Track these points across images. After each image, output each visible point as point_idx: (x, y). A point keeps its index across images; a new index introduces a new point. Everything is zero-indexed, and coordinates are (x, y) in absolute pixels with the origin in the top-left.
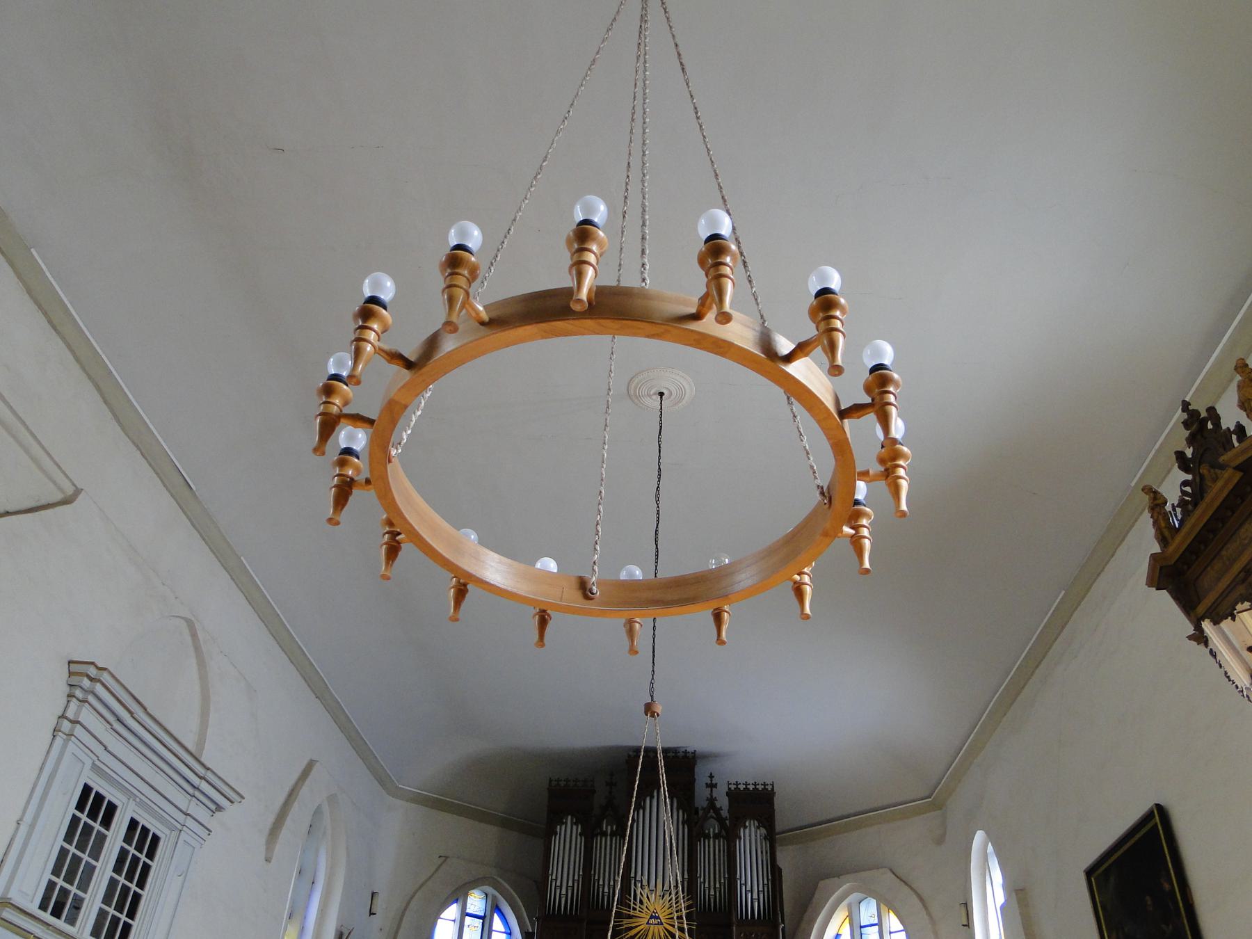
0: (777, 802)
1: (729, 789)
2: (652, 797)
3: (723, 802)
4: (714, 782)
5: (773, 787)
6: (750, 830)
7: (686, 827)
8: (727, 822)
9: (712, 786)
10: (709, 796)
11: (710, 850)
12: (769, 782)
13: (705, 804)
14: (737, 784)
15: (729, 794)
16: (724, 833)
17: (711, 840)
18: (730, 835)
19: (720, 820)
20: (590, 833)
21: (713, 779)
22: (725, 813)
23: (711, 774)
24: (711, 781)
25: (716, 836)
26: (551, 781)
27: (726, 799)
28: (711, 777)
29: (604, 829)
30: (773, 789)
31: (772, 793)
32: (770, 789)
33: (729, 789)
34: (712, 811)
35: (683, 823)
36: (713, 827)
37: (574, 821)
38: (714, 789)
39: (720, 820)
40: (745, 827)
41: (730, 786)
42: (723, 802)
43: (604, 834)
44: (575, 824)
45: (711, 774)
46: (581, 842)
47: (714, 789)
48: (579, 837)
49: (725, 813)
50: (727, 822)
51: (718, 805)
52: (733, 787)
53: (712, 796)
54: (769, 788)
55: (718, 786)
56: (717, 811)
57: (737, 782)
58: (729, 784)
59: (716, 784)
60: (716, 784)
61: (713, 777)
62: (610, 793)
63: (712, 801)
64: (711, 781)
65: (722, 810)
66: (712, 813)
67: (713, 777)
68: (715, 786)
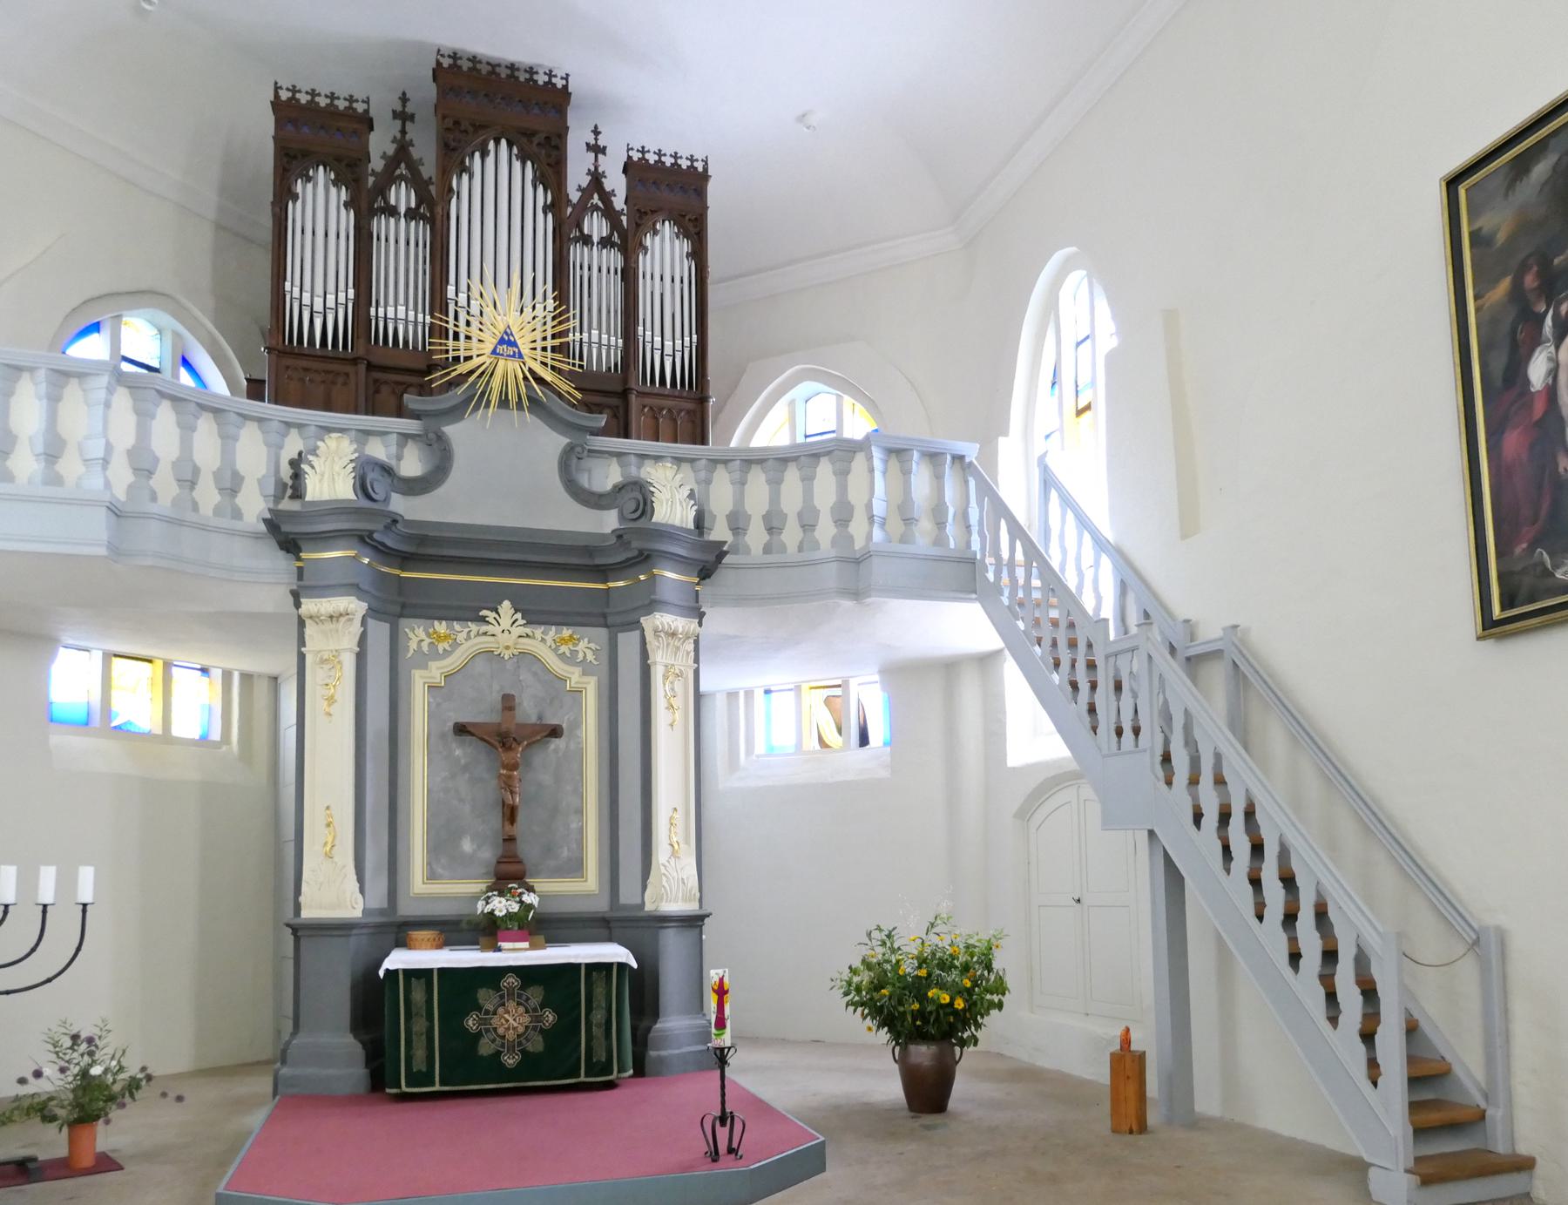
0: (713, 190)
1: (630, 158)
2: (484, 155)
3: (616, 183)
4: (601, 143)
5: (706, 163)
6: (662, 240)
7: (550, 216)
8: (624, 219)
9: (597, 150)
10: (593, 169)
12: (699, 156)
13: (585, 181)
14: (643, 151)
15: (628, 167)
16: (616, 238)
17: (595, 248)
18: (627, 242)
19: (609, 213)
21: (600, 137)
22: (619, 203)
23: (596, 127)
24: (596, 139)
25: (605, 243)
26: (277, 88)
27: (622, 179)
28: (596, 132)
29: (393, 202)
30: (706, 169)
31: (704, 177)
32: (700, 169)
33: (630, 158)
34: (596, 196)
35: (545, 213)
36: (596, 226)
37: (332, 176)
38: (600, 156)
39: (609, 213)
40: (655, 233)
41: (631, 153)
42: (616, 183)
43: (392, 211)
44: (336, 183)
45: (596, 127)
46: (348, 219)
47: (600, 156)
48: (342, 208)
49: (619, 203)
50: (624, 219)
51: (608, 185)
52: (636, 156)
53: (596, 168)
54: (699, 166)
55: (608, 151)
56: (606, 197)
57: (643, 147)
58: (628, 150)
59: (605, 148)
60: (605, 148)
61: (600, 133)
62: (403, 132)
63: (596, 178)
64: (596, 139)
65: (615, 196)
66: (596, 199)
67: (600, 133)
68: (603, 150)
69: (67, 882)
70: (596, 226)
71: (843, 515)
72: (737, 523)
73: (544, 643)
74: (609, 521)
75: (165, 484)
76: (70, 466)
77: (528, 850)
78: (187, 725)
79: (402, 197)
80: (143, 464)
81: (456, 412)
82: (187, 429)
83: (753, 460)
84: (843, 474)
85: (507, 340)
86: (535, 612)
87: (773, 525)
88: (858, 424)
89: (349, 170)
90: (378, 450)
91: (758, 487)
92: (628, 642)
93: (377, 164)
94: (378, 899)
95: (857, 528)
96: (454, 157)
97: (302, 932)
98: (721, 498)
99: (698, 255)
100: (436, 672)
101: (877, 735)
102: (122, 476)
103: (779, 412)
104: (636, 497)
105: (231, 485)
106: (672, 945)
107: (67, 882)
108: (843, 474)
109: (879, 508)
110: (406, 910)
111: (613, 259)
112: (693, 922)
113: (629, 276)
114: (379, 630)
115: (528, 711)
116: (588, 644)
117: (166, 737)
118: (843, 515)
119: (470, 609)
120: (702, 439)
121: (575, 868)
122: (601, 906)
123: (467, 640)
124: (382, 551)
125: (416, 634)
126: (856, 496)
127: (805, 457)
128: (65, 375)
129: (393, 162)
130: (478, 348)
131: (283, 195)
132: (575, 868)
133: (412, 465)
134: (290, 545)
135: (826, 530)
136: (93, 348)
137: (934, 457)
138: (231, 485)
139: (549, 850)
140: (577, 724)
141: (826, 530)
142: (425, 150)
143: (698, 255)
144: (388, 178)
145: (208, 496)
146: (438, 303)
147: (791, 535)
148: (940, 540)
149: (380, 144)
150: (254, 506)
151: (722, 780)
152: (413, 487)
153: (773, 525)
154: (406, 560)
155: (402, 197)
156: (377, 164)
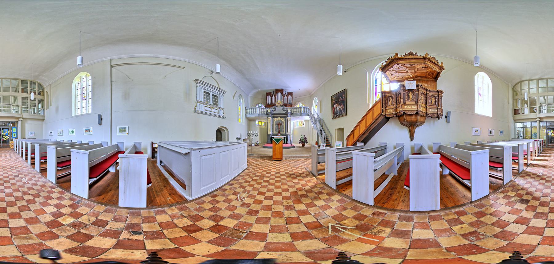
11: (285, 98)
18: (287, 97)
20: (271, 97)
42: (287, 94)
69: (257, 132)
70: (285, 96)
71: (300, 111)
72: (294, 112)
73: (281, 119)
74: (286, 112)
75: (261, 112)
76: (256, 112)
77: (280, 131)
78: (263, 125)
79: (273, 96)
80: (260, 112)
81: (276, 107)
82: (262, 109)
83: (296, 108)
84: (300, 109)
85: (279, 103)
86: (281, 117)
87: (296, 112)
88: (304, 106)
89: (270, 95)
90: (272, 109)
91: (295, 110)
92: (286, 119)
93: (272, 95)
94: (272, 133)
95: (301, 112)
96: (276, 94)
97: (268, 135)
98: (293, 110)
99: (292, 97)
100: (275, 121)
101: (304, 124)
102: (259, 112)
103: (298, 105)
104: (287, 111)
105: (264, 112)
106: (289, 136)
107: (257, 132)
108: (300, 109)
109: (302, 111)
110: (274, 134)
111: (287, 97)
112: (290, 135)
113: (287, 98)
114: (272, 119)
115: (280, 123)
116: (284, 119)
117: (261, 125)
118: (300, 111)
119: (277, 117)
120: (292, 107)
121: (283, 132)
122: (285, 134)
123: (277, 119)
124: (272, 115)
125: (274, 119)
126: (301, 110)
127: (298, 108)
128: (256, 108)
129: (273, 95)
130: (277, 103)
131: (267, 97)
132: (283, 132)
133: (274, 110)
134: (267, 115)
135: (299, 112)
136: (257, 106)
137: (306, 108)
138: (264, 112)
139: (282, 131)
140: (283, 124)
141: (299, 112)
142: (275, 93)
143: (292, 97)
144: (273, 95)
145: (263, 113)
146: (276, 101)
147: (297, 112)
148: (307, 113)
149: (272, 94)
150: (265, 113)
151: (295, 127)
152: (274, 111)
153: (296, 112)
154: (273, 115)
155: (273, 96)
156: (272, 95)
